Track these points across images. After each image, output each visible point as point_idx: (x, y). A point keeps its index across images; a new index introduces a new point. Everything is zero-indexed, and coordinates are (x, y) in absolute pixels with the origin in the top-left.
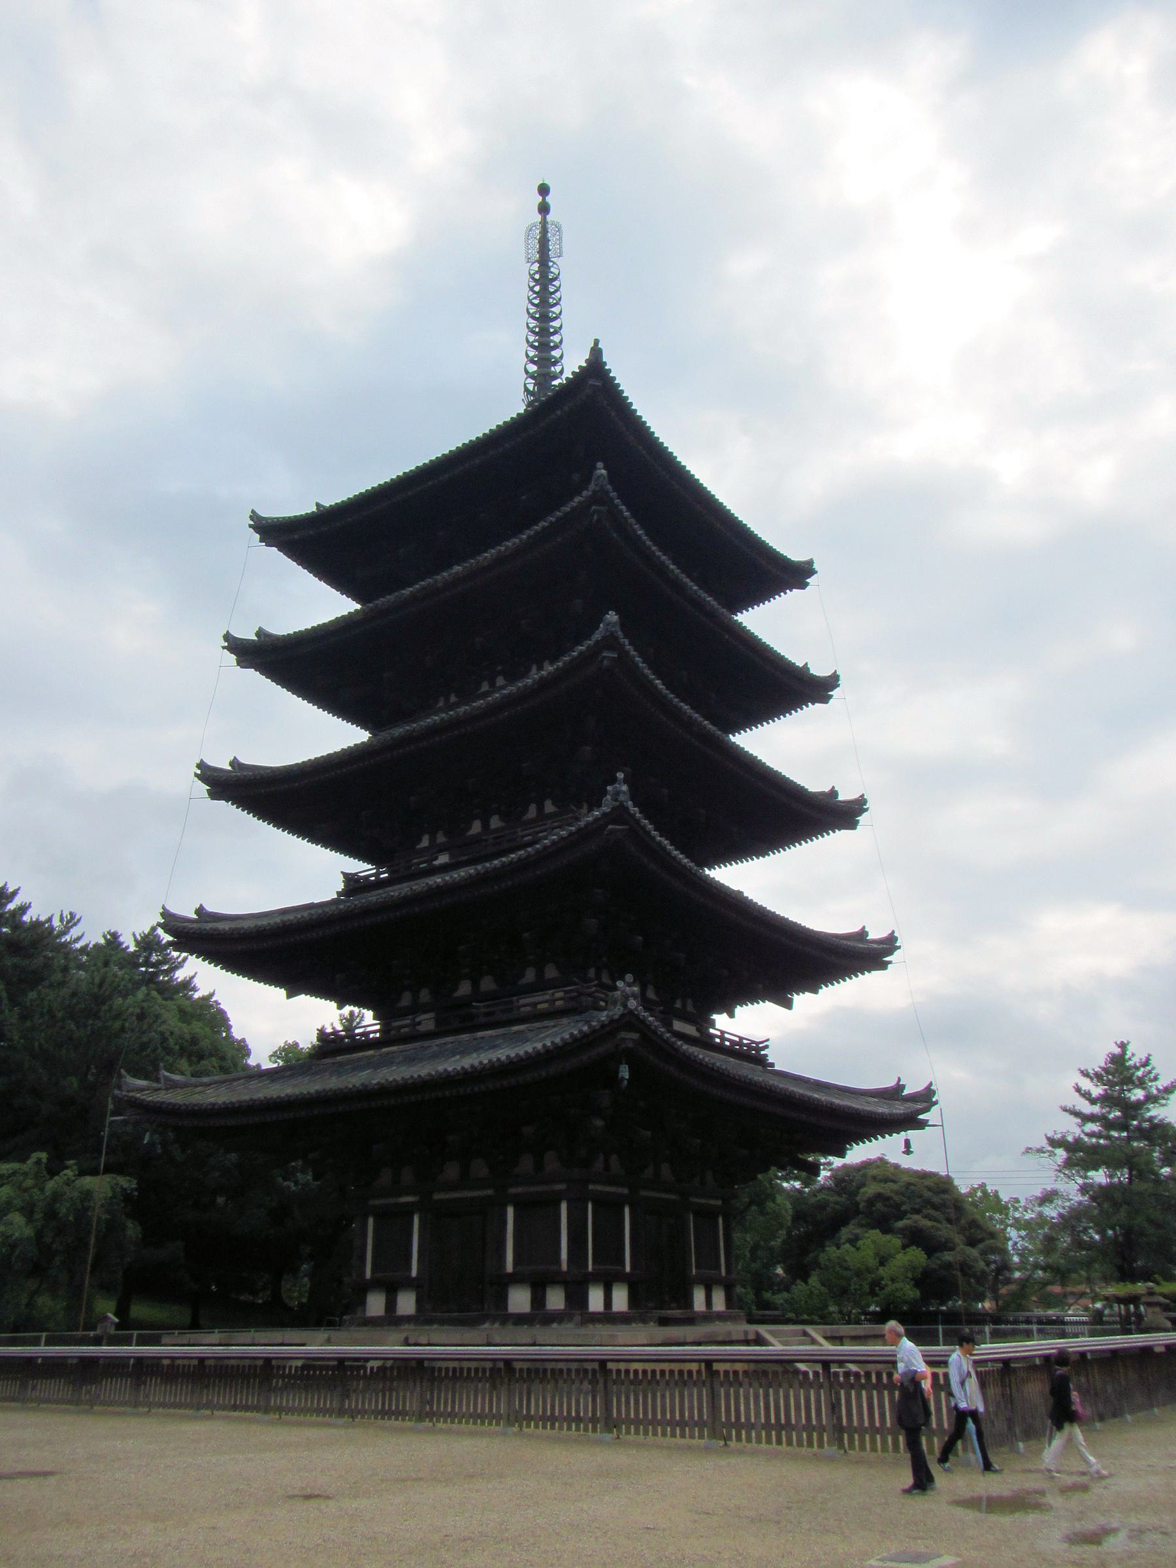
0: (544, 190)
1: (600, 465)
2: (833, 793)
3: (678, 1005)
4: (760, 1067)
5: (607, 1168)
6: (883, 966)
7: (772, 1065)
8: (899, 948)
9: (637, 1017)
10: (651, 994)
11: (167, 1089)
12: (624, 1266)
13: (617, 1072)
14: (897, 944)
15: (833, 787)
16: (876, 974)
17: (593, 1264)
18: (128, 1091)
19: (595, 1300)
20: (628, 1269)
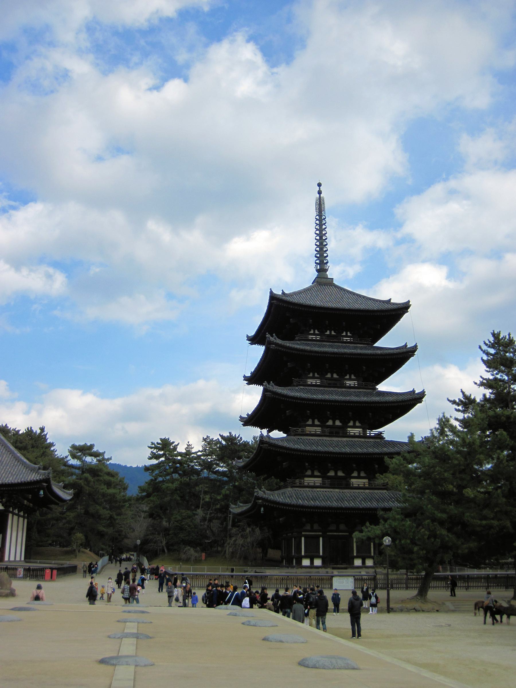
0: (319, 185)
1: (267, 333)
2: (414, 391)
3: (355, 474)
4: (386, 491)
9: (258, 496)
10: (340, 474)
11: (238, 508)
12: (319, 553)
13: (260, 510)
15: (414, 389)
18: (231, 508)
19: (306, 562)
20: (321, 554)
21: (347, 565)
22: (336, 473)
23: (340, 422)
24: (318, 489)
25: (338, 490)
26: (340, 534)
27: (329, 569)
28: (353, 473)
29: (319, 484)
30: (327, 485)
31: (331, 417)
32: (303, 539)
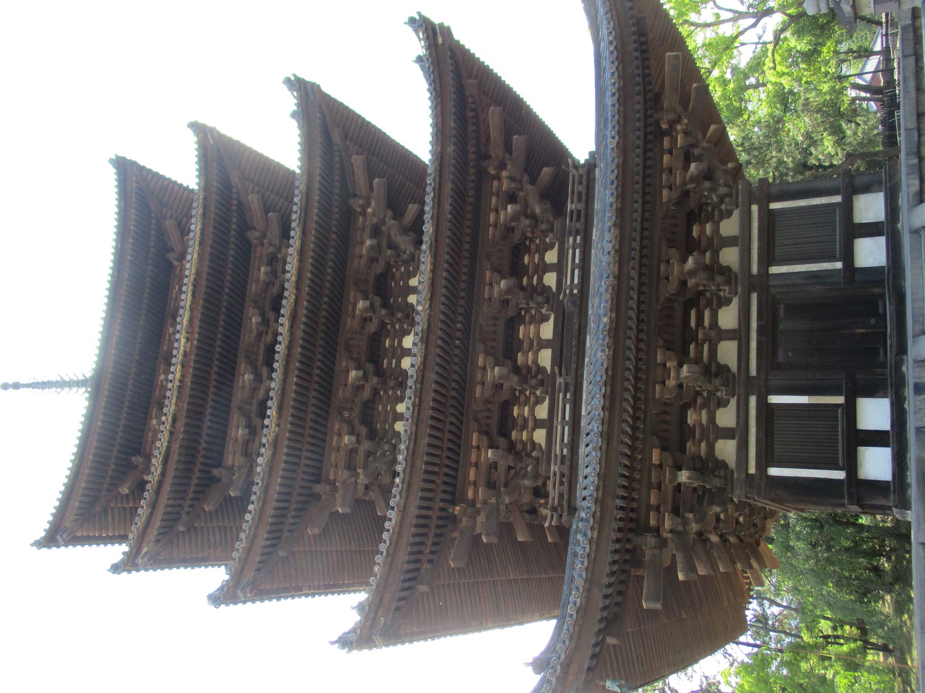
2: (294, 115)
3: (550, 279)
4: (597, 171)
5: (728, 434)
6: (446, 32)
7: (592, 154)
8: (419, 14)
14: (418, 18)
16: (457, 35)
17: (834, 467)
20: (840, 400)
21: (882, 296)
22: (543, 344)
23: (409, 334)
24: (583, 413)
25: (588, 337)
26: (754, 324)
27: (904, 368)
28: (549, 287)
29: (568, 406)
30: (570, 380)
31: (394, 361)
32: (774, 471)
